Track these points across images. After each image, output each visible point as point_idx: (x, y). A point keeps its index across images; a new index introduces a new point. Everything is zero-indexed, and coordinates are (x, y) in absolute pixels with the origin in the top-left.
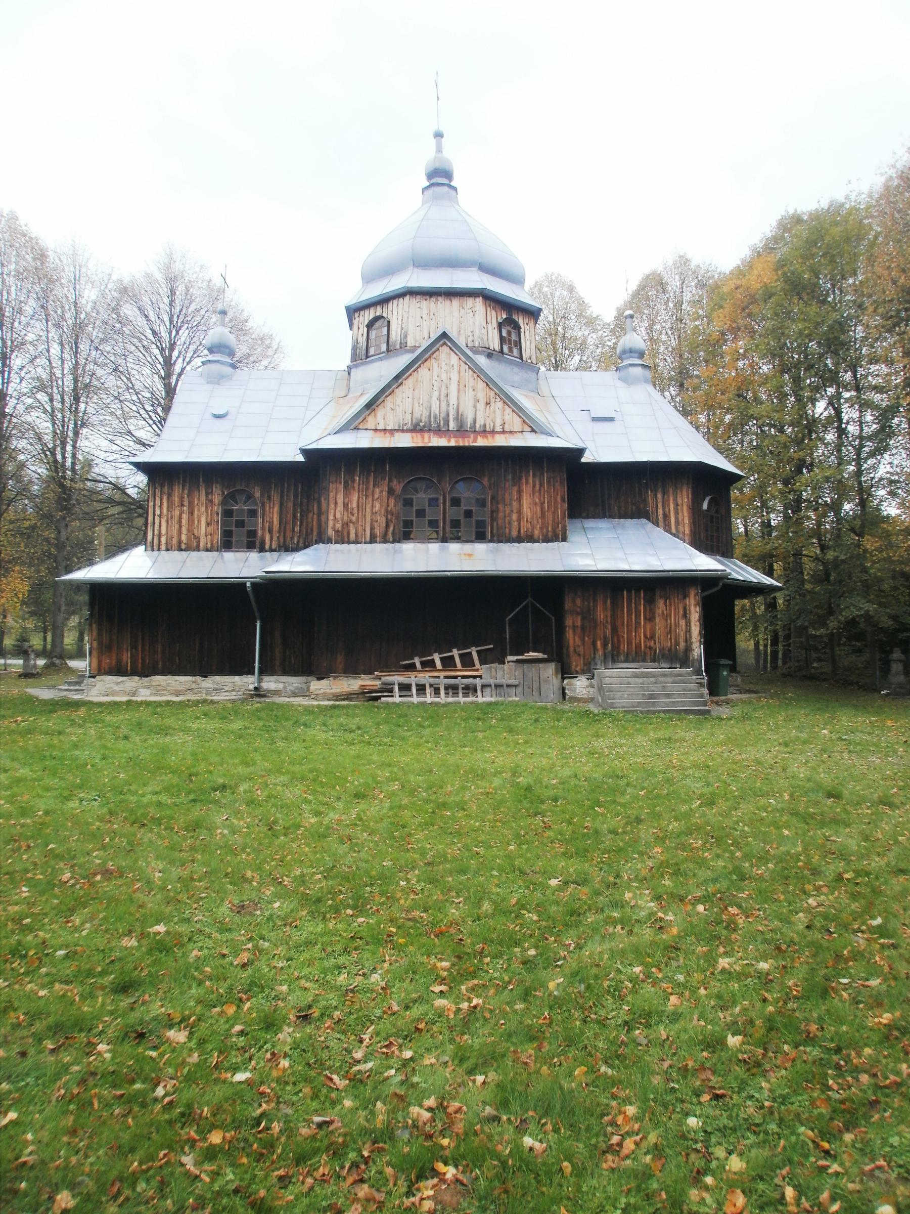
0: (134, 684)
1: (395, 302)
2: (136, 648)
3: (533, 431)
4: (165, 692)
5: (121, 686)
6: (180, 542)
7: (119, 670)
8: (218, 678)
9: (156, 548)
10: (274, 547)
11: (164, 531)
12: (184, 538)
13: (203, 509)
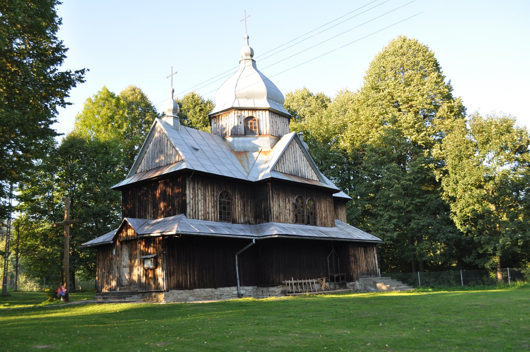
0: (186, 295)
1: (261, 112)
2: (186, 274)
3: (320, 181)
4: (200, 298)
5: (181, 295)
7: (179, 287)
8: (221, 289)
13: (210, 199)
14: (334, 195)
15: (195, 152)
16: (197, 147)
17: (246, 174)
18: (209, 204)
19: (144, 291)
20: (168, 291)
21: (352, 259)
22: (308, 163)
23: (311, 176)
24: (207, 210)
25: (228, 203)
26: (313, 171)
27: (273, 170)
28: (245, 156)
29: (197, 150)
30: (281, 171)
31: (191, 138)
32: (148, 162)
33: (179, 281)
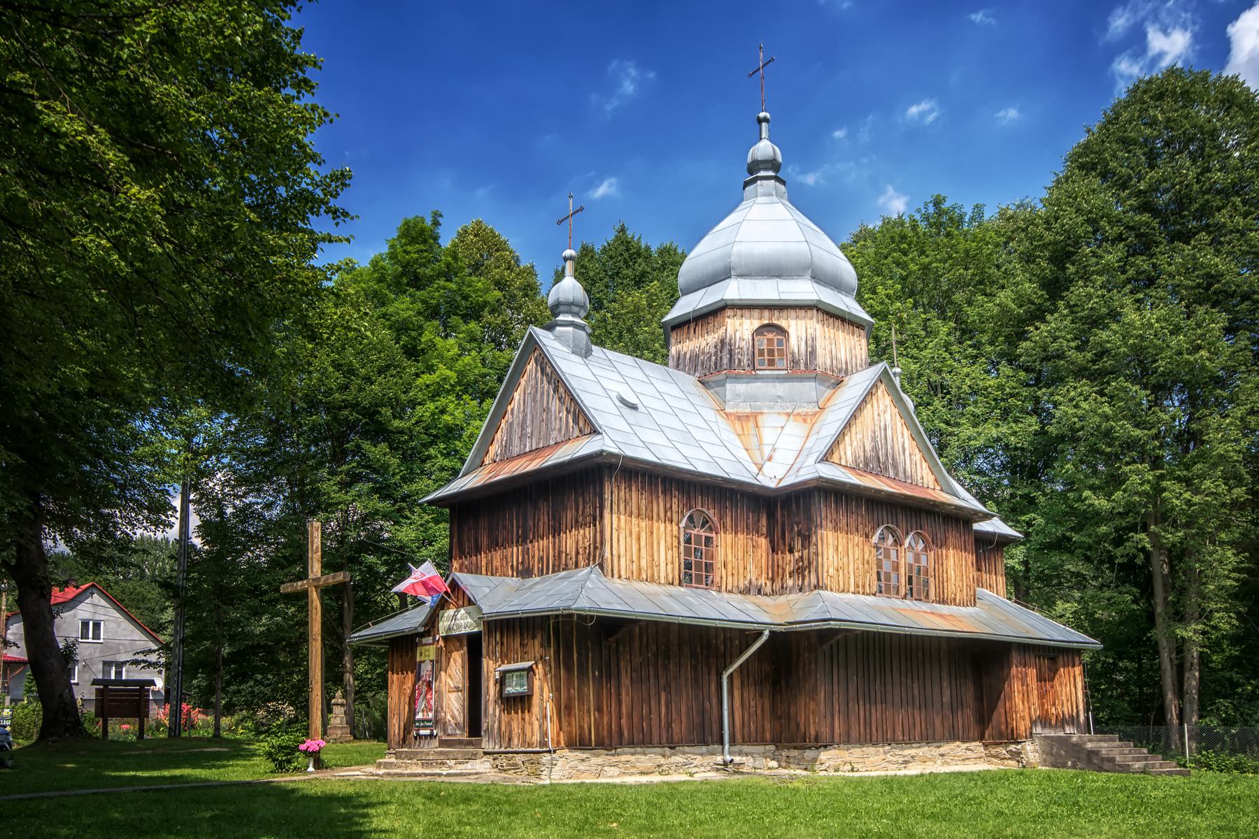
5: (586, 763)
6: (640, 569)
7: (578, 743)
9: (616, 575)
10: (729, 588)
11: (622, 552)
12: (643, 563)
14: (977, 526)
15: (626, 411)
16: (632, 399)
17: (755, 470)
18: (659, 543)
19: (497, 749)
20: (555, 752)
21: (1017, 686)
22: (914, 443)
23: (919, 475)
24: (656, 558)
25: (708, 540)
26: (924, 465)
27: (826, 458)
28: (751, 424)
29: (633, 407)
30: (843, 463)
31: (616, 376)
32: (510, 439)
33: (581, 728)
